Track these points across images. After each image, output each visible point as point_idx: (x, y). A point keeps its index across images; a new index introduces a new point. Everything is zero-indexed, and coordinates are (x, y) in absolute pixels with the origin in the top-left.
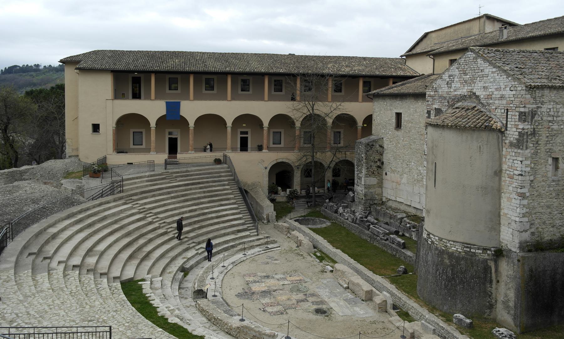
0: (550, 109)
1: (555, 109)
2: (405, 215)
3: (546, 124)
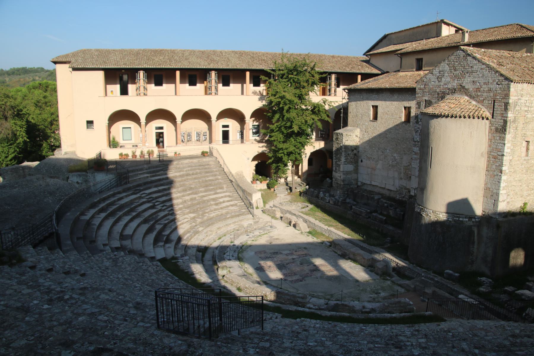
2: (380, 196)
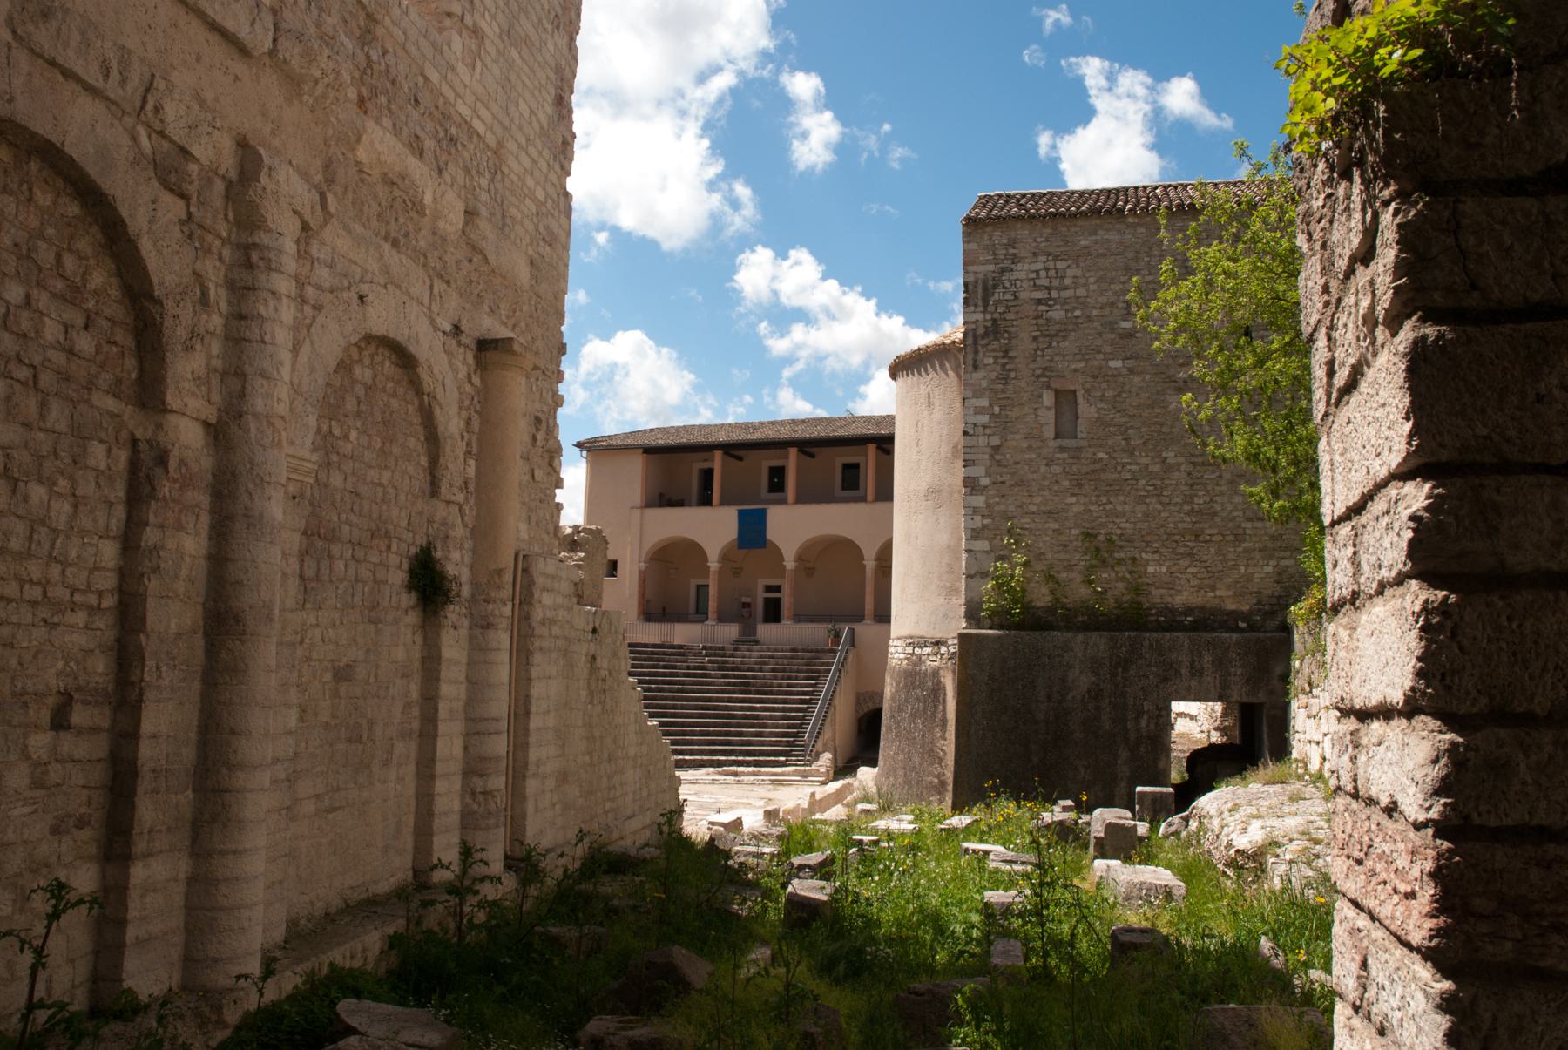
0: (1037, 272)
1: (1052, 273)
3: (1029, 309)
